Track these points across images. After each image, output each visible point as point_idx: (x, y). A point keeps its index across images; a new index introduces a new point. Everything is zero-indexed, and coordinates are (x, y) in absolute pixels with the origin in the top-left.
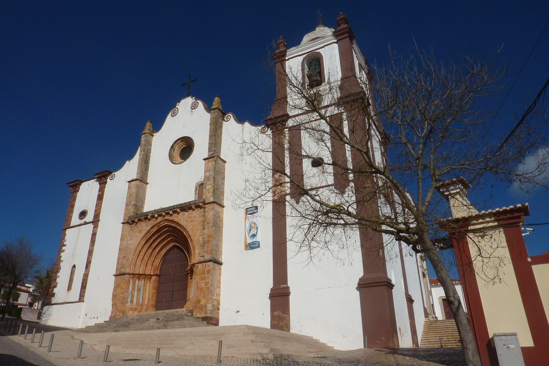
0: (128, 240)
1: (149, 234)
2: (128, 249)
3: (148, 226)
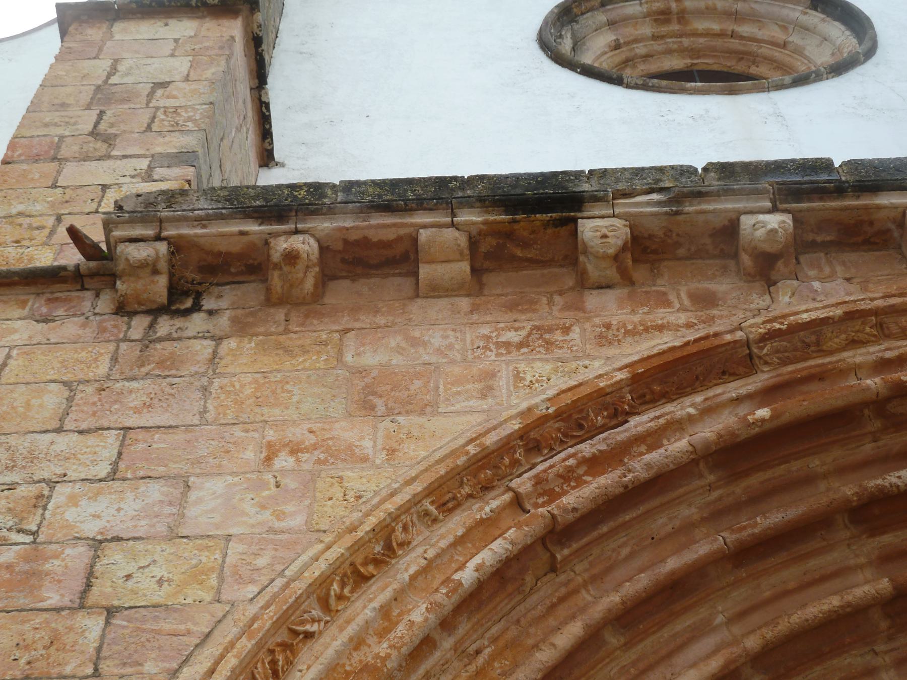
0: (52, 484)
1: (595, 464)
2: (53, 598)
3: (549, 344)
